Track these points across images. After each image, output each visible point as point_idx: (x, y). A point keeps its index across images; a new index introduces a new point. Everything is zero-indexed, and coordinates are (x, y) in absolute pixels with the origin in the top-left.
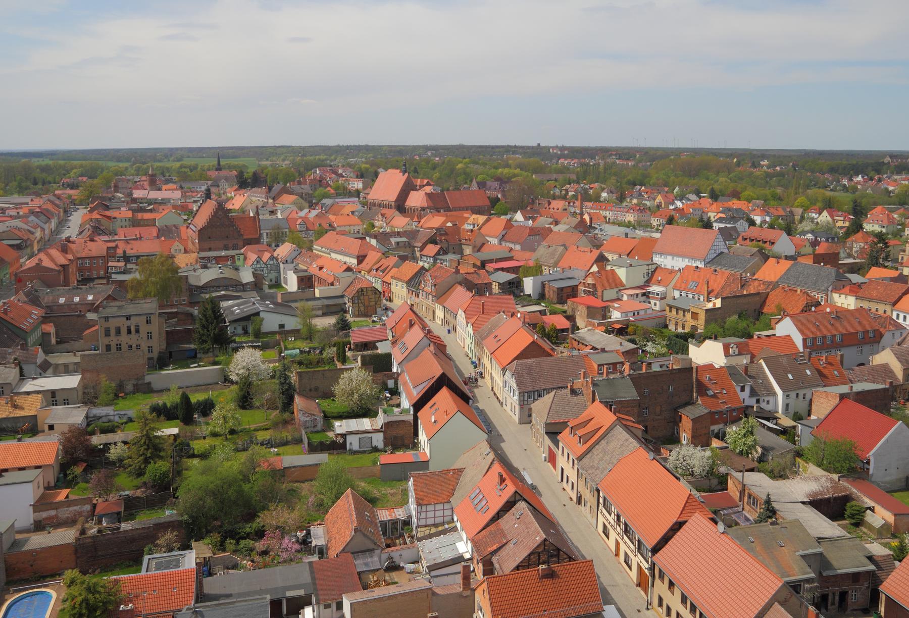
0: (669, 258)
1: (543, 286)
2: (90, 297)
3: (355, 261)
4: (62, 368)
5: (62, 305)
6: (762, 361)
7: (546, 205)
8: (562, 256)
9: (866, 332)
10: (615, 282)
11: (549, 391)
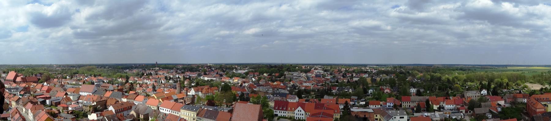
10: (69, 99)
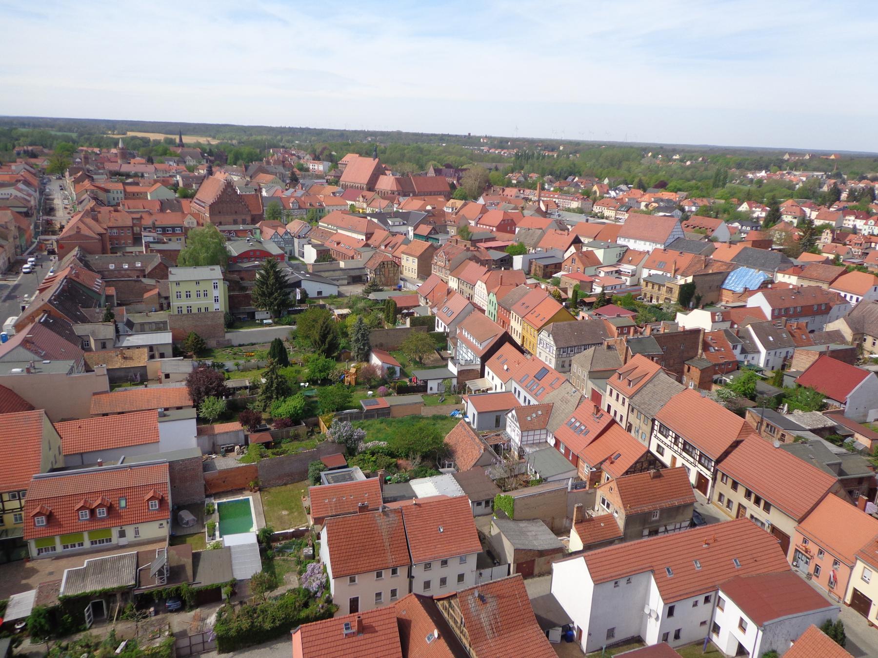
0: (632, 241)
1: (531, 263)
2: (139, 265)
3: (364, 238)
4: (139, 326)
5: (112, 271)
6: (749, 327)
7: (501, 192)
8: (541, 238)
9: (819, 305)
11: (586, 346)
